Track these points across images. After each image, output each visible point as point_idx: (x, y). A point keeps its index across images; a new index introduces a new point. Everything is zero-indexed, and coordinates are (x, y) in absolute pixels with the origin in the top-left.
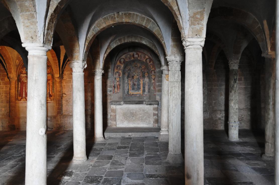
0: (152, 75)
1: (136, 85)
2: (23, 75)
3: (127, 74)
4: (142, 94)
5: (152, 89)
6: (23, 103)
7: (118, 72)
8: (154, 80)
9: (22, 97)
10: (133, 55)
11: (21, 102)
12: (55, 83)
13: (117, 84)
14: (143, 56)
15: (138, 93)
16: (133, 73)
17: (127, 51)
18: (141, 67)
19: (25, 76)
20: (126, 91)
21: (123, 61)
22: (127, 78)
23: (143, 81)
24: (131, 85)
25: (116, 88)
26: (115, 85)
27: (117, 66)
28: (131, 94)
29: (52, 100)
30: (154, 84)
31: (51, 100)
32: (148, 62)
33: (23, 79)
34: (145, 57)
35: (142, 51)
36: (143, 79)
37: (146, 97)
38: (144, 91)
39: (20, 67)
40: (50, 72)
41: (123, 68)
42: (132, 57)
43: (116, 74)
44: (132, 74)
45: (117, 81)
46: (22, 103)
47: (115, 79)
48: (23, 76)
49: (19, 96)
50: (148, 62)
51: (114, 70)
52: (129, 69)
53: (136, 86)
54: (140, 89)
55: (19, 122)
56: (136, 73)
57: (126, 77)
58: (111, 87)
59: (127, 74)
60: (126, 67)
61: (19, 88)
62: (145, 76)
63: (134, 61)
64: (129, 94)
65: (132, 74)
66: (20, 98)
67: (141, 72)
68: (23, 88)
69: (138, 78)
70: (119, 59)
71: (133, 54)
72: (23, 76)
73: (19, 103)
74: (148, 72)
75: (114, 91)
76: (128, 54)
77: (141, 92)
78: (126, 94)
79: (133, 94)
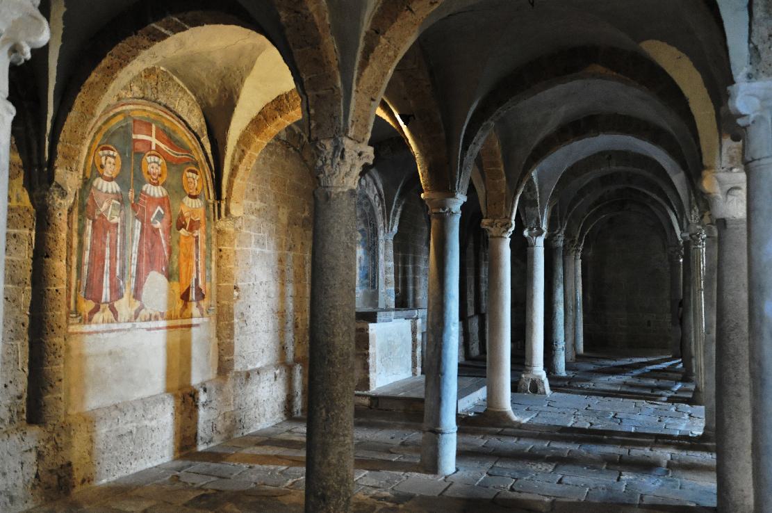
2: (105, 183)
6: (103, 332)
9: (98, 301)
11: (93, 327)
12: (214, 239)
14: (371, 184)
19: (113, 193)
29: (205, 313)
31: (202, 316)
33: (105, 205)
39: (93, 141)
40: (200, 189)
46: (97, 332)
48: (104, 190)
49: (86, 298)
50: (377, 204)
55: (91, 440)
61: (87, 254)
66: (90, 305)
68: (104, 252)
72: (107, 192)
73: (82, 333)
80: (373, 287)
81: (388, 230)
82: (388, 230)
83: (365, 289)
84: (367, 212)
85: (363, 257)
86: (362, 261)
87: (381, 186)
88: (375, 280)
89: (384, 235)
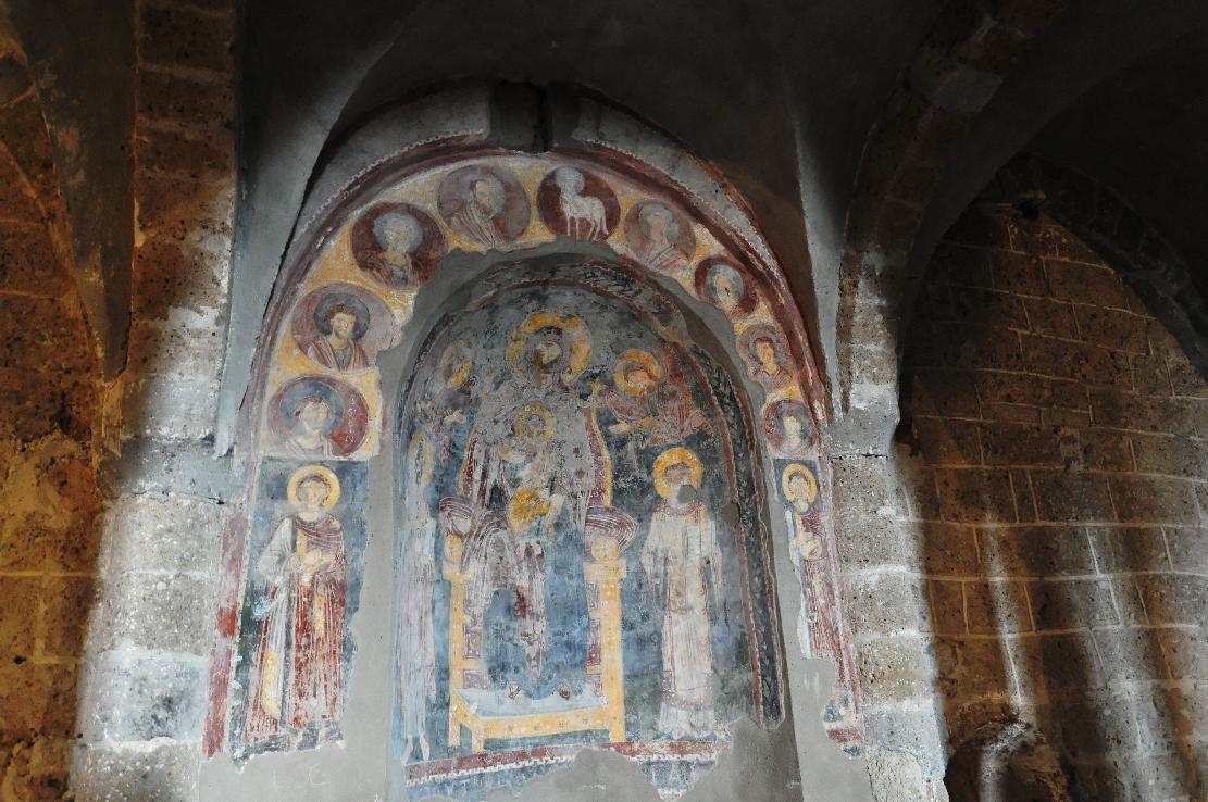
0: (790, 469)
1: (540, 609)
3: (430, 449)
4: (617, 735)
5: (807, 651)
7: (320, 388)
8: (811, 524)
10: (549, 197)
13: (292, 582)
14: (661, 217)
15: (574, 723)
16: (493, 450)
17: (477, 128)
18: (611, 384)
20: (420, 687)
21: (404, 248)
22: (436, 508)
23: (632, 551)
24: (467, 602)
25: (275, 652)
26: (253, 595)
27: (308, 301)
28: (477, 747)
30: (817, 581)
32: (722, 297)
34: (685, 244)
35: (654, 157)
36: (629, 537)
37: (695, 775)
38: (647, 686)
41: (407, 329)
42: (535, 211)
43: (285, 416)
44: (488, 458)
45: (299, 525)
47: (276, 488)
50: (728, 302)
51: (266, 346)
52: (465, 389)
53: (540, 627)
54: (592, 669)
56: (532, 455)
57: (425, 480)
58: (174, 618)
59: (429, 448)
60: (446, 320)
62: (651, 486)
63: (541, 275)
64: (454, 740)
65: (488, 458)
67: (601, 441)
69: (564, 511)
70: (356, 214)
71: (552, 176)
74: (696, 441)
75: (231, 702)
76: (487, 171)
77: (600, 703)
78: (417, 755)
79: (499, 735)
80: (773, 707)
81: (829, 411)
82: (829, 411)
83: (740, 717)
84: (688, 345)
85: (718, 560)
86: (717, 580)
87: (738, 221)
88: (772, 660)
89: (810, 438)
